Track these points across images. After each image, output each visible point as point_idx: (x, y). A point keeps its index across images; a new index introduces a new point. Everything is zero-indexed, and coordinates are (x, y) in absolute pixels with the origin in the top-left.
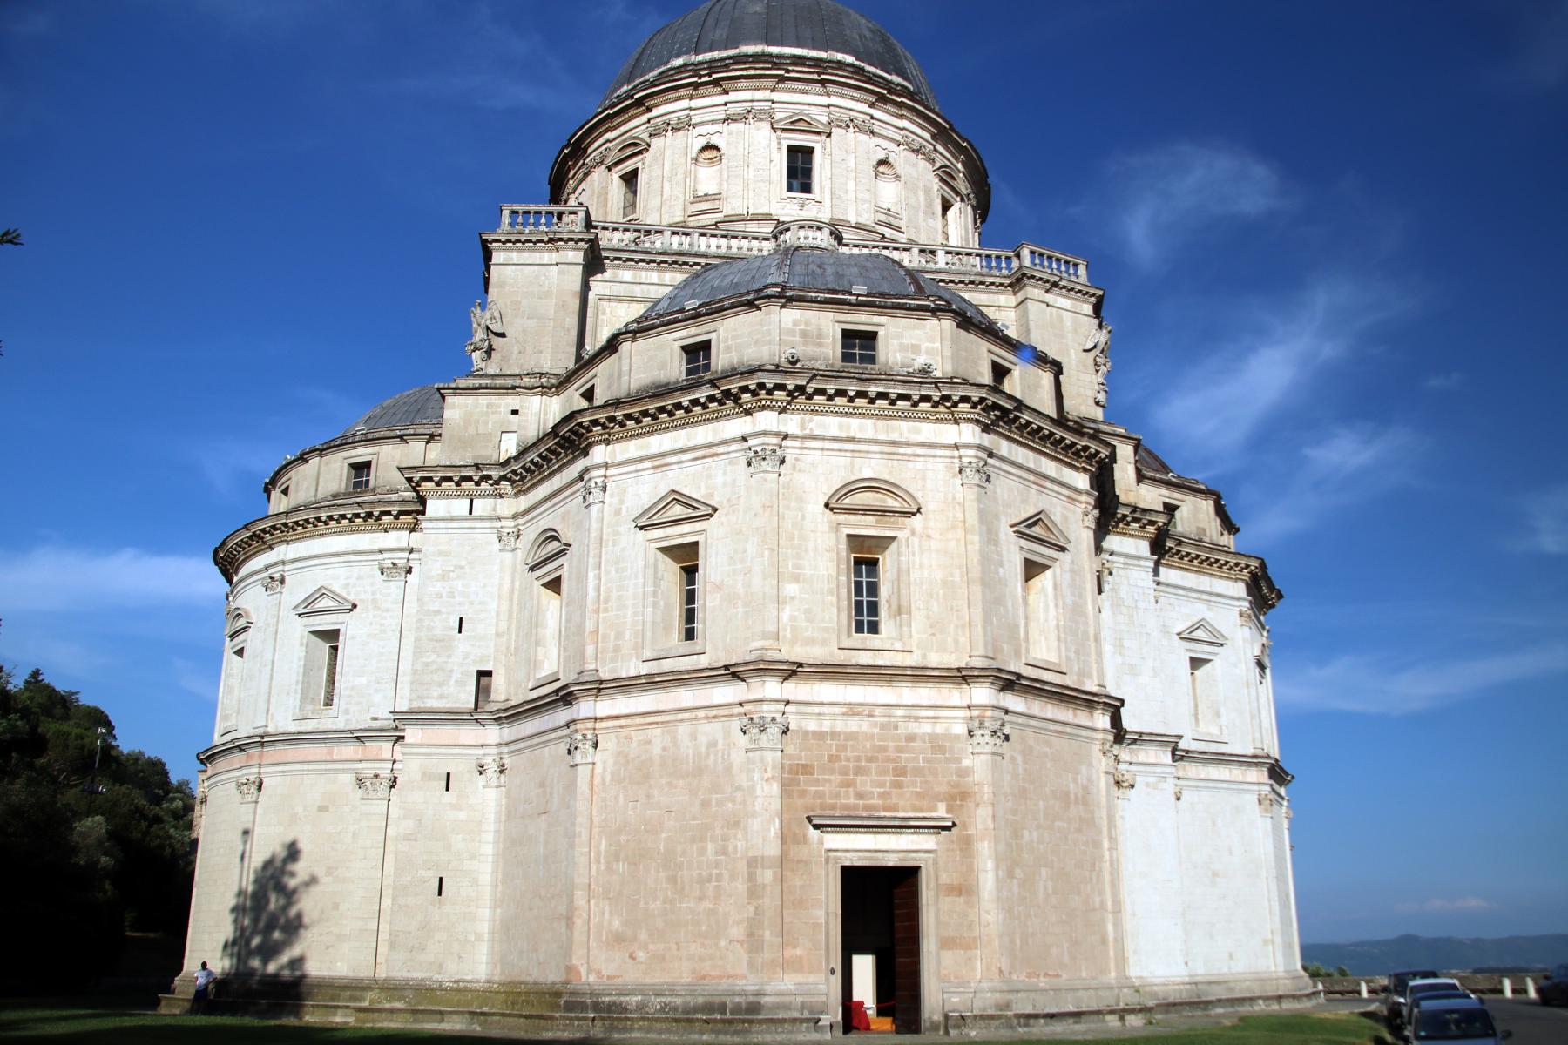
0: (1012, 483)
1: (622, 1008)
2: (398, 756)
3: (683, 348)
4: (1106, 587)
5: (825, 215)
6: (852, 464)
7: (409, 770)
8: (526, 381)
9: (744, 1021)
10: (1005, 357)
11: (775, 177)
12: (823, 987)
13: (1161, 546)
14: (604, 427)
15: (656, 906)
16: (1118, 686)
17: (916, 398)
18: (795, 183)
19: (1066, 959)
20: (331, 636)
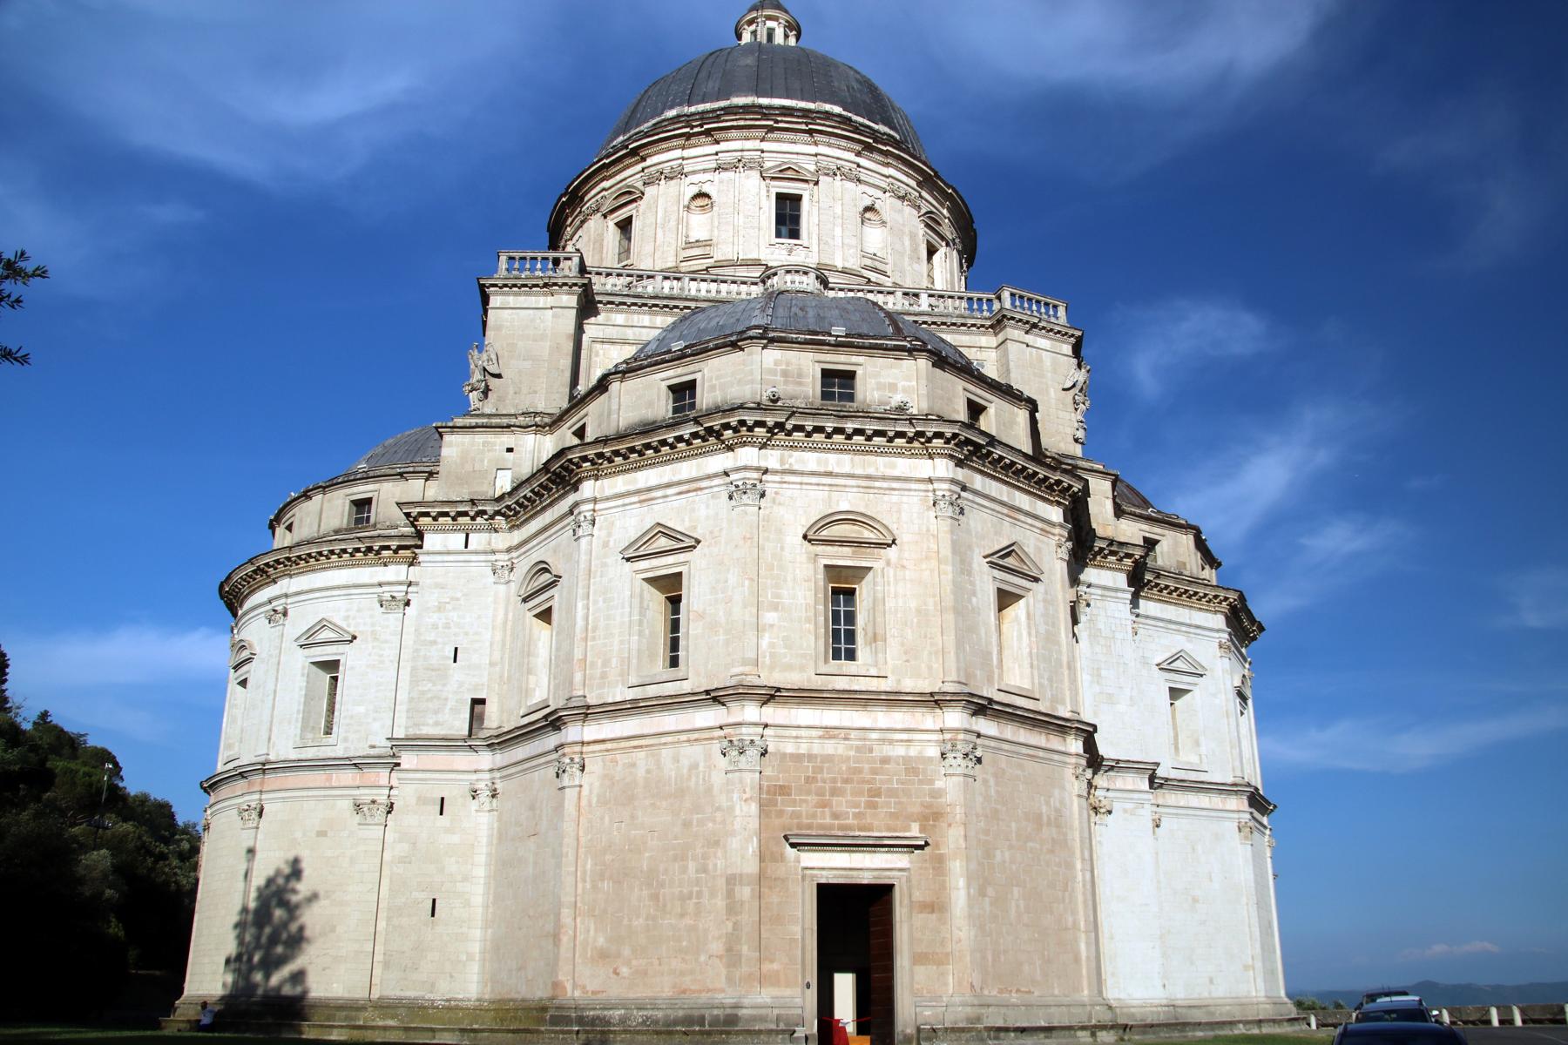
0: (986, 516)
1: (606, 1022)
2: (394, 783)
3: (670, 387)
4: (1083, 618)
5: (812, 261)
7: (405, 794)
8: (521, 420)
9: (722, 1033)
10: (981, 395)
11: (764, 224)
12: (798, 1001)
13: (1140, 579)
14: (593, 463)
15: (639, 922)
16: (1096, 714)
17: (891, 434)
18: (784, 230)
20: (331, 666)
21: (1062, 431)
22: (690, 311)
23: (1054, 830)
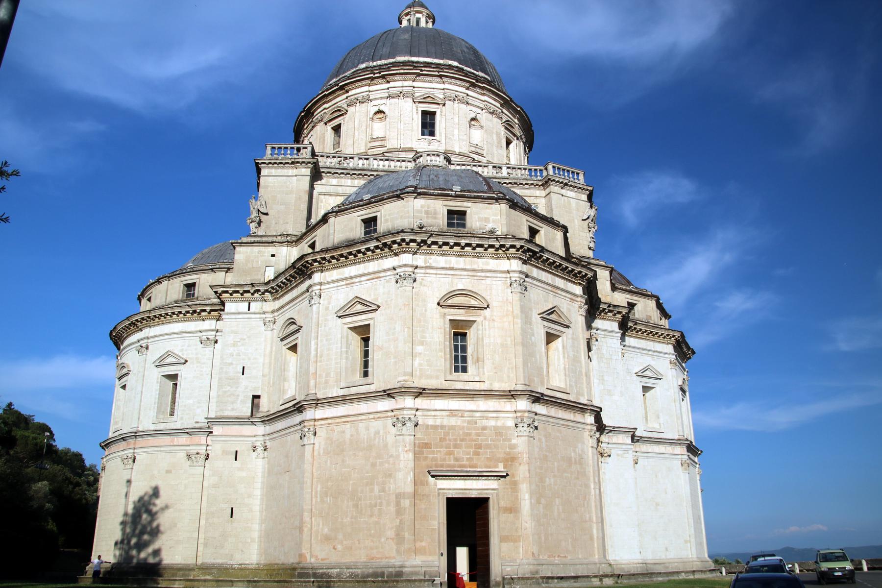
0: (539, 291)
1: (329, 576)
2: (209, 442)
3: (362, 220)
4: (594, 348)
5: (442, 148)
7: (215, 449)
8: (279, 239)
9: (393, 581)
10: (536, 224)
11: (415, 128)
12: (436, 563)
13: (625, 326)
14: (320, 263)
15: (347, 520)
16: (601, 402)
17: (486, 246)
18: (426, 131)
19: (570, 548)
20: (173, 377)
21: (582, 243)
22: (374, 177)
23: (578, 466)
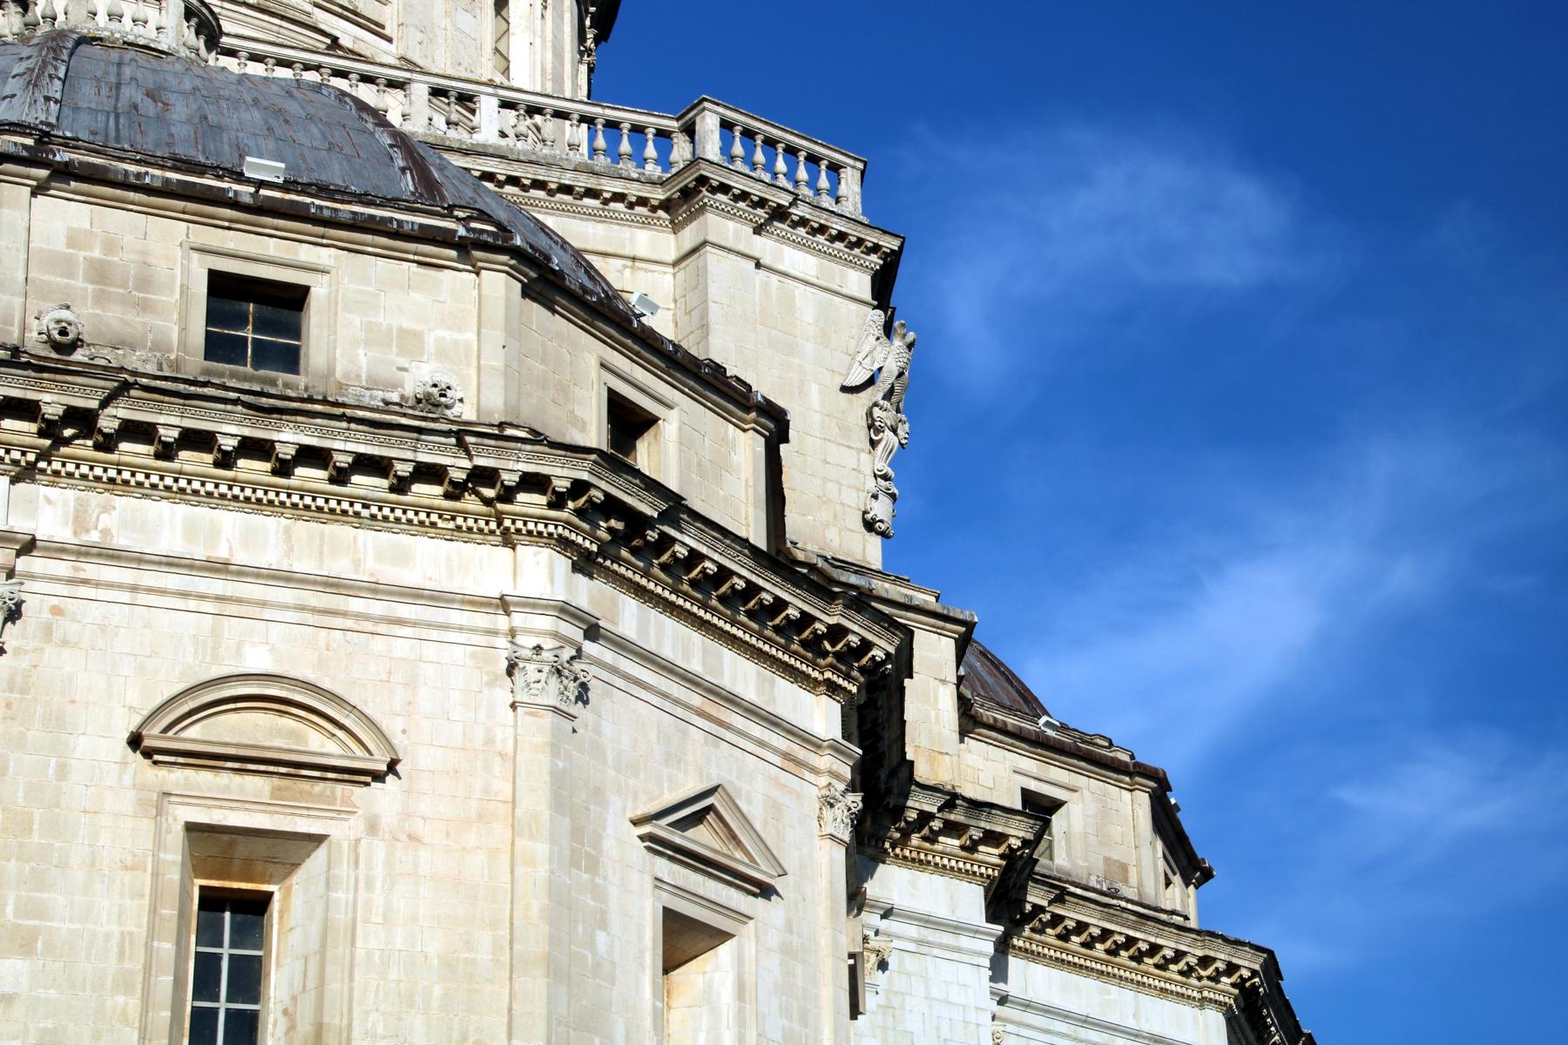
4: (869, 1001)
6: (216, 633)
10: (646, 385)
13: (1018, 900)
